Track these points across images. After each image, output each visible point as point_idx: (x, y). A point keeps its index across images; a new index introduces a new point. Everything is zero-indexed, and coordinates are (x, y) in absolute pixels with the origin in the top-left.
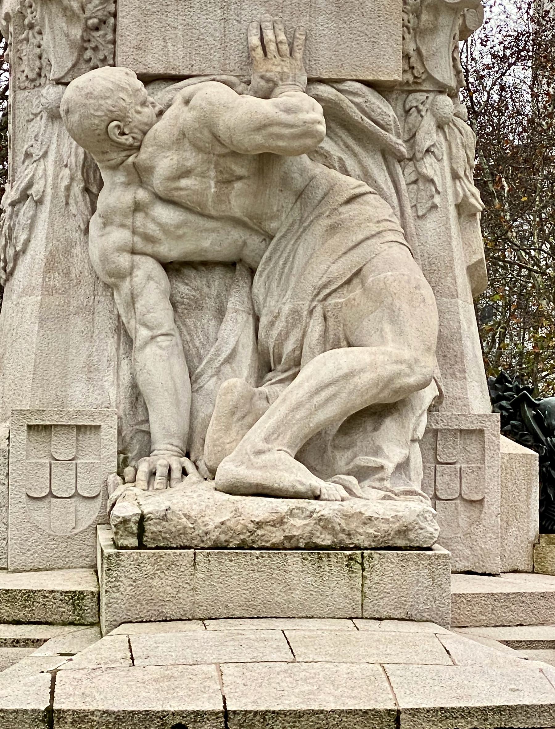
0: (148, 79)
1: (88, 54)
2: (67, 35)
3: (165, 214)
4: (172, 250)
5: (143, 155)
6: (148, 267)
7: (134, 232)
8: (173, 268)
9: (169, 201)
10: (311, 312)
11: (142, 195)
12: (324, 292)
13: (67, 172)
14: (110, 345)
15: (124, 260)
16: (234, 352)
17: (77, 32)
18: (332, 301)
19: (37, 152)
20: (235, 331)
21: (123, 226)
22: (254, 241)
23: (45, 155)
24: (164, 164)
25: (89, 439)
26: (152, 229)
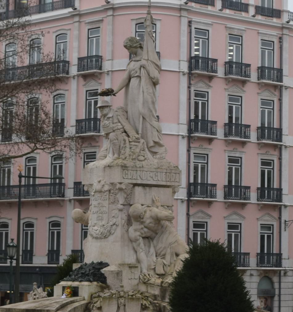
0: (142, 205)
1: (126, 200)
2: (124, 196)
3: (146, 230)
4: (144, 236)
5: (144, 220)
6: (141, 239)
7: (141, 233)
8: (143, 238)
9: (145, 227)
10: (168, 247)
11: (143, 226)
12: (170, 244)
13: (124, 221)
14: (132, 252)
15: (138, 237)
16: (152, 254)
17: (125, 196)
18: (172, 245)
19: (116, 216)
20: (152, 250)
21: (139, 231)
22: (154, 234)
23: (118, 217)
24: (148, 221)
25: (136, 269)
26: (143, 232)
